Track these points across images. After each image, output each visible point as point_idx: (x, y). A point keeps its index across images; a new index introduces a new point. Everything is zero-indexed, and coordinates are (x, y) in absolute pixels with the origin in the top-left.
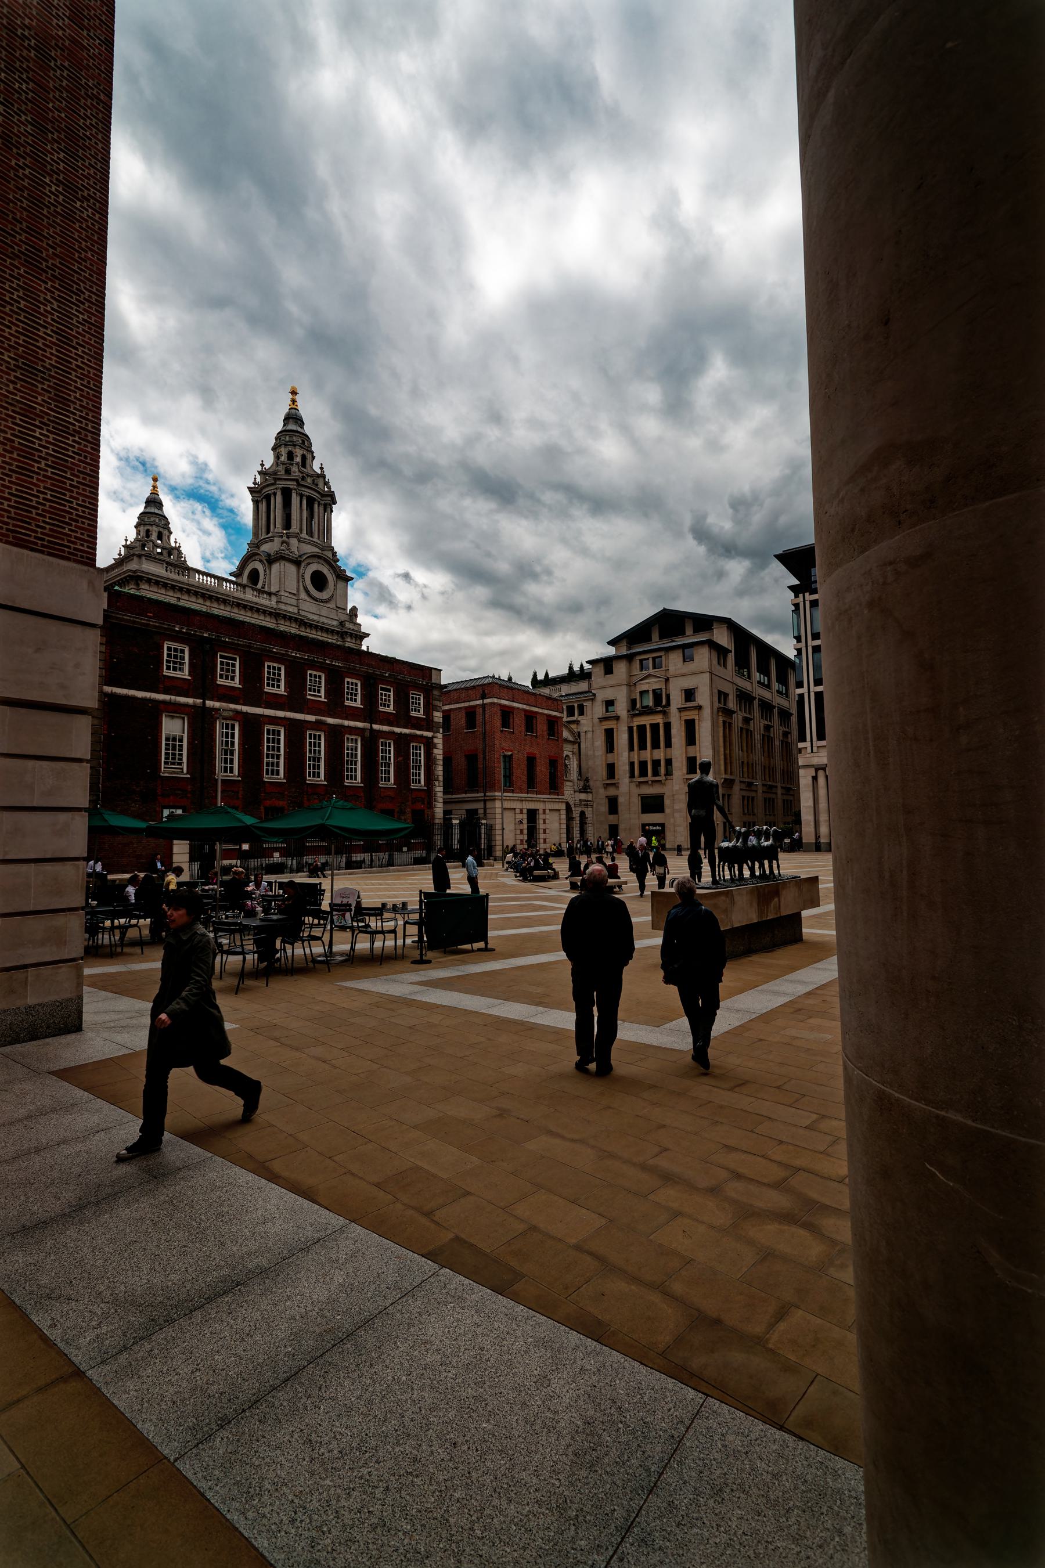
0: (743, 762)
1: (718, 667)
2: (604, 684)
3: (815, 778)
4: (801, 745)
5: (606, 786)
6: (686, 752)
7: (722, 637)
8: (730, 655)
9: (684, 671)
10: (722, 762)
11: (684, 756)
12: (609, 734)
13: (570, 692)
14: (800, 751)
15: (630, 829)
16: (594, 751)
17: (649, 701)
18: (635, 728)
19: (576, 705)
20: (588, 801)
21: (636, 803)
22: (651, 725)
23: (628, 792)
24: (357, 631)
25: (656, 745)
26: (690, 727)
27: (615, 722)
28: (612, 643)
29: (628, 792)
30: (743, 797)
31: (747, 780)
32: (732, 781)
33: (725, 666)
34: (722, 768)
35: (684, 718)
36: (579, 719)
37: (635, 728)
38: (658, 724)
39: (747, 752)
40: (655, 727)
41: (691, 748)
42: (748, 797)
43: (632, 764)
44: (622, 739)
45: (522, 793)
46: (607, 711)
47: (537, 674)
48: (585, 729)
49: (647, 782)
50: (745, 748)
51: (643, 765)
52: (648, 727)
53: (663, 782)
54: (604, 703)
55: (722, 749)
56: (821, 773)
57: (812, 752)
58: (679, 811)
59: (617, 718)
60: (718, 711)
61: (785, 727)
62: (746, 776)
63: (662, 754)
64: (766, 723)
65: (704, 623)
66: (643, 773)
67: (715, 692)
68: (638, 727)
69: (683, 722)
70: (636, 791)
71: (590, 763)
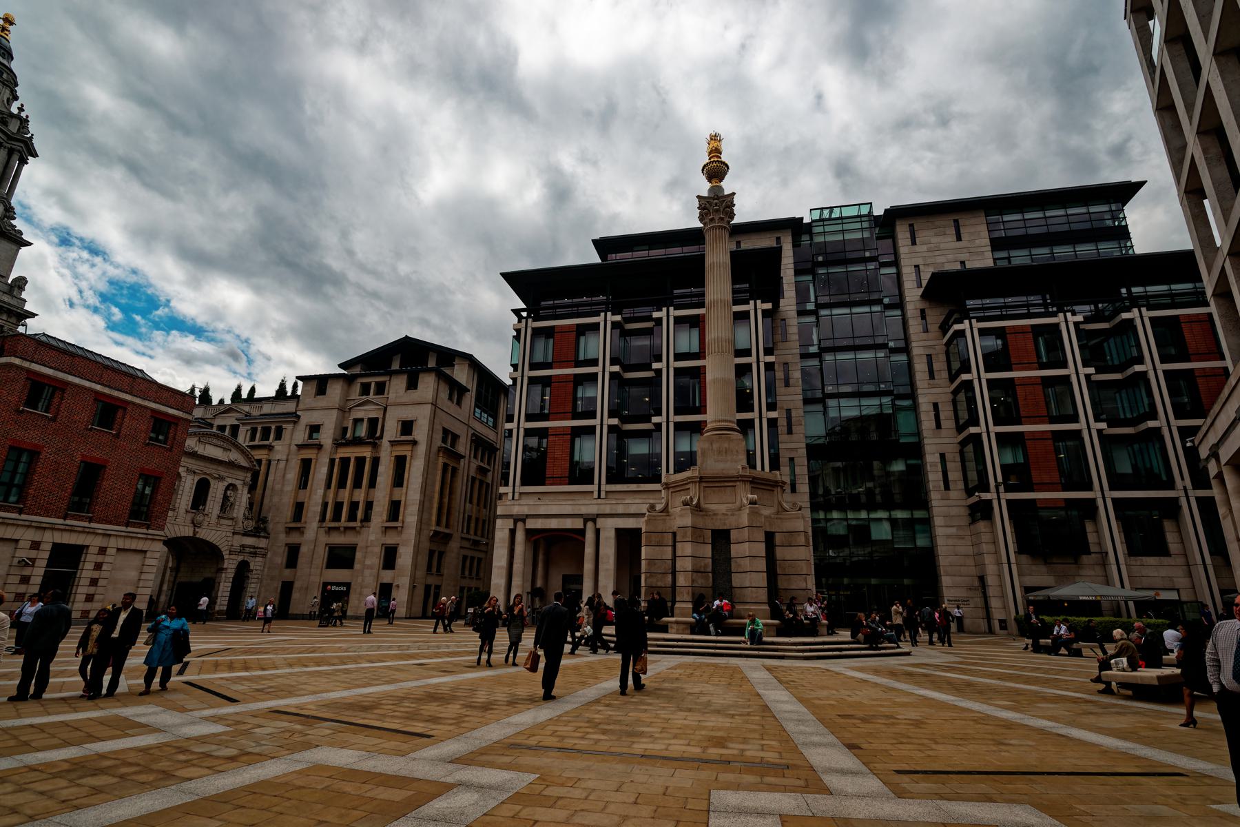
0: (470, 517)
1: (449, 403)
2: (314, 405)
3: (513, 532)
4: (502, 490)
5: (289, 530)
6: (391, 494)
7: (461, 374)
8: (468, 395)
9: (405, 399)
10: (435, 511)
11: (387, 499)
12: (306, 465)
13: (273, 412)
14: (500, 496)
15: (307, 588)
16: (283, 485)
17: (362, 431)
18: (337, 461)
19: (273, 427)
20: (258, 548)
21: (322, 554)
22: (357, 459)
23: (315, 540)
24: (18, 308)
25: (357, 484)
26: (400, 464)
27: (315, 451)
28: (341, 366)
29: (315, 540)
30: (465, 558)
31: (472, 537)
32: (447, 538)
33: (459, 403)
34: (434, 518)
35: (395, 454)
36: (273, 444)
37: (337, 461)
38: (364, 458)
39: (478, 504)
40: (360, 461)
41: (397, 490)
42: (472, 558)
43: (325, 505)
44: (320, 472)
45: (47, 516)
46: (310, 437)
47: (243, 388)
48: (278, 457)
49: (337, 529)
50: (475, 501)
51: (338, 506)
52: (352, 461)
53: (358, 529)
54: (308, 427)
55: (437, 496)
56: (520, 525)
57: (513, 499)
58: (370, 567)
59: (319, 447)
60: (439, 451)
61: (482, 461)
62: (472, 532)
63: (363, 495)
64: (482, 464)
65: (448, 356)
66: (337, 517)
67: (439, 429)
68: (341, 459)
69: (393, 459)
70: (324, 539)
71: (276, 499)
